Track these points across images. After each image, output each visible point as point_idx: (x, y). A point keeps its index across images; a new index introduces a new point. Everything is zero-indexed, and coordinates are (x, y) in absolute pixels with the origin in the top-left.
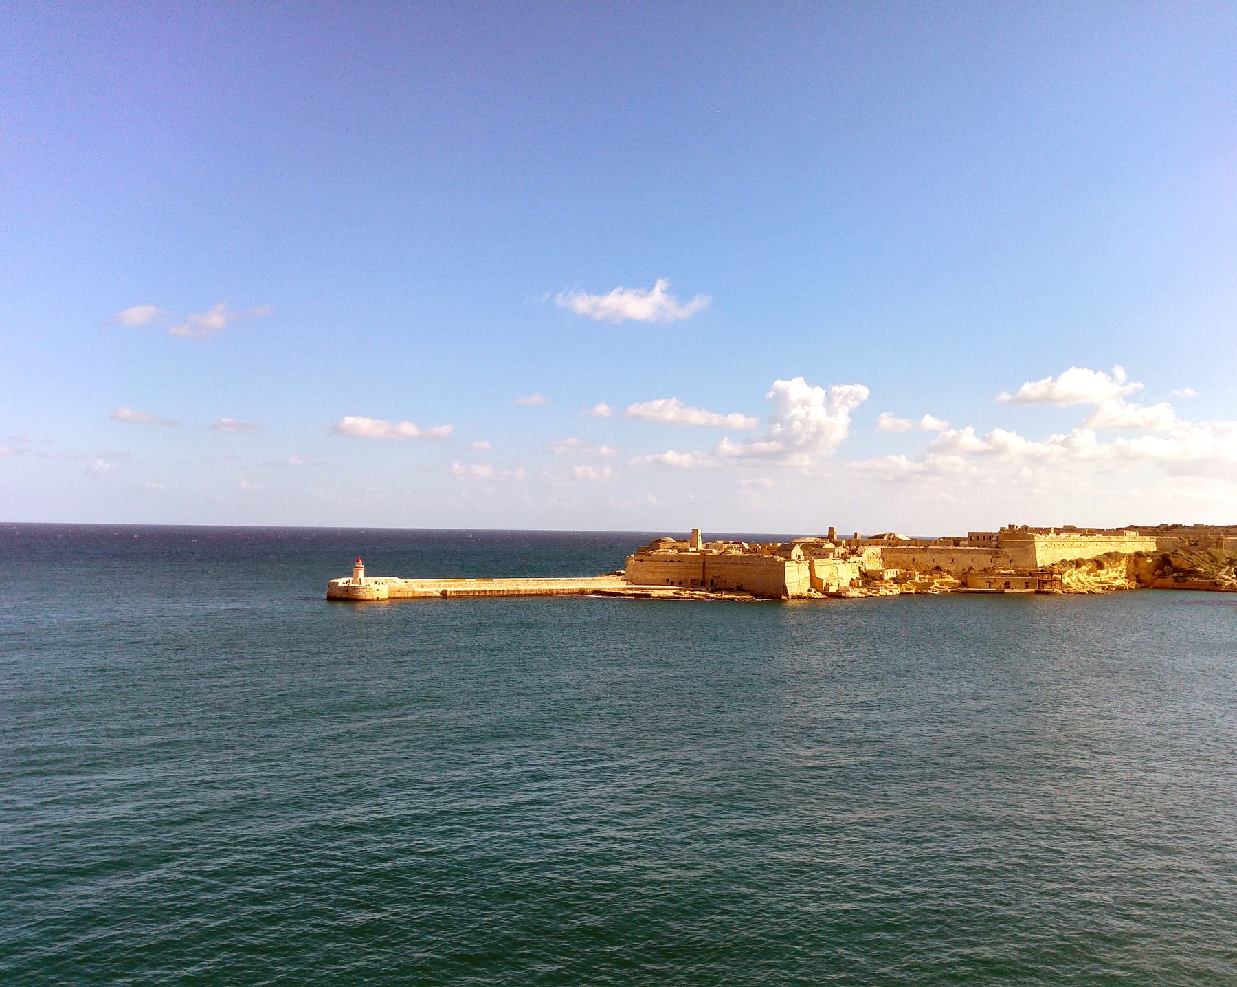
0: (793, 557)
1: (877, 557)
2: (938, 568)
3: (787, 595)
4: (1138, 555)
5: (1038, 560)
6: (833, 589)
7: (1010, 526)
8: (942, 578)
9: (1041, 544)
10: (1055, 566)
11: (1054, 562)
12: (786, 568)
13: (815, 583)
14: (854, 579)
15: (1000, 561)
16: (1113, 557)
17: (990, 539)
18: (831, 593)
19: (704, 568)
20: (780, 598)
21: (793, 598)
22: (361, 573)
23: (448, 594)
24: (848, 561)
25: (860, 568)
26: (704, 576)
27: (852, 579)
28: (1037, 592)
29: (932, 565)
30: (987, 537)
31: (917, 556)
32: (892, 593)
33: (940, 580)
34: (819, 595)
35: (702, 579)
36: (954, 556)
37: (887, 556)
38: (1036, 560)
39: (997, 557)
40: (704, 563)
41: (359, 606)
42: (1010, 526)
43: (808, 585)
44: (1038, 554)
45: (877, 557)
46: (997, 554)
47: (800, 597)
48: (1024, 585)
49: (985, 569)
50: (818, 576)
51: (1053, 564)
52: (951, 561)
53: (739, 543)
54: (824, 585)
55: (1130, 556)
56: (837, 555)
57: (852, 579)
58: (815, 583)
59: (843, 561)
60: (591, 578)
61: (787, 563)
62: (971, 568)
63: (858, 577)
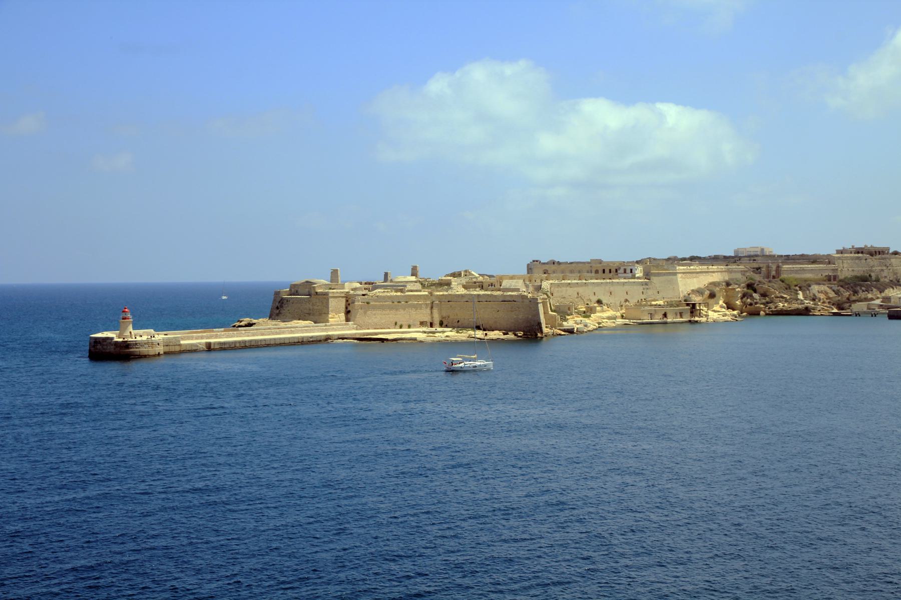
15: (650, 292)
17: (616, 271)
22: (130, 328)
23: (212, 347)
26: (432, 318)
30: (613, 270)
31: (581, 290)
35: (427, 319)
36: (612, 289)
39: (647, 289)
41: (135, 366)
60: (324, 324)
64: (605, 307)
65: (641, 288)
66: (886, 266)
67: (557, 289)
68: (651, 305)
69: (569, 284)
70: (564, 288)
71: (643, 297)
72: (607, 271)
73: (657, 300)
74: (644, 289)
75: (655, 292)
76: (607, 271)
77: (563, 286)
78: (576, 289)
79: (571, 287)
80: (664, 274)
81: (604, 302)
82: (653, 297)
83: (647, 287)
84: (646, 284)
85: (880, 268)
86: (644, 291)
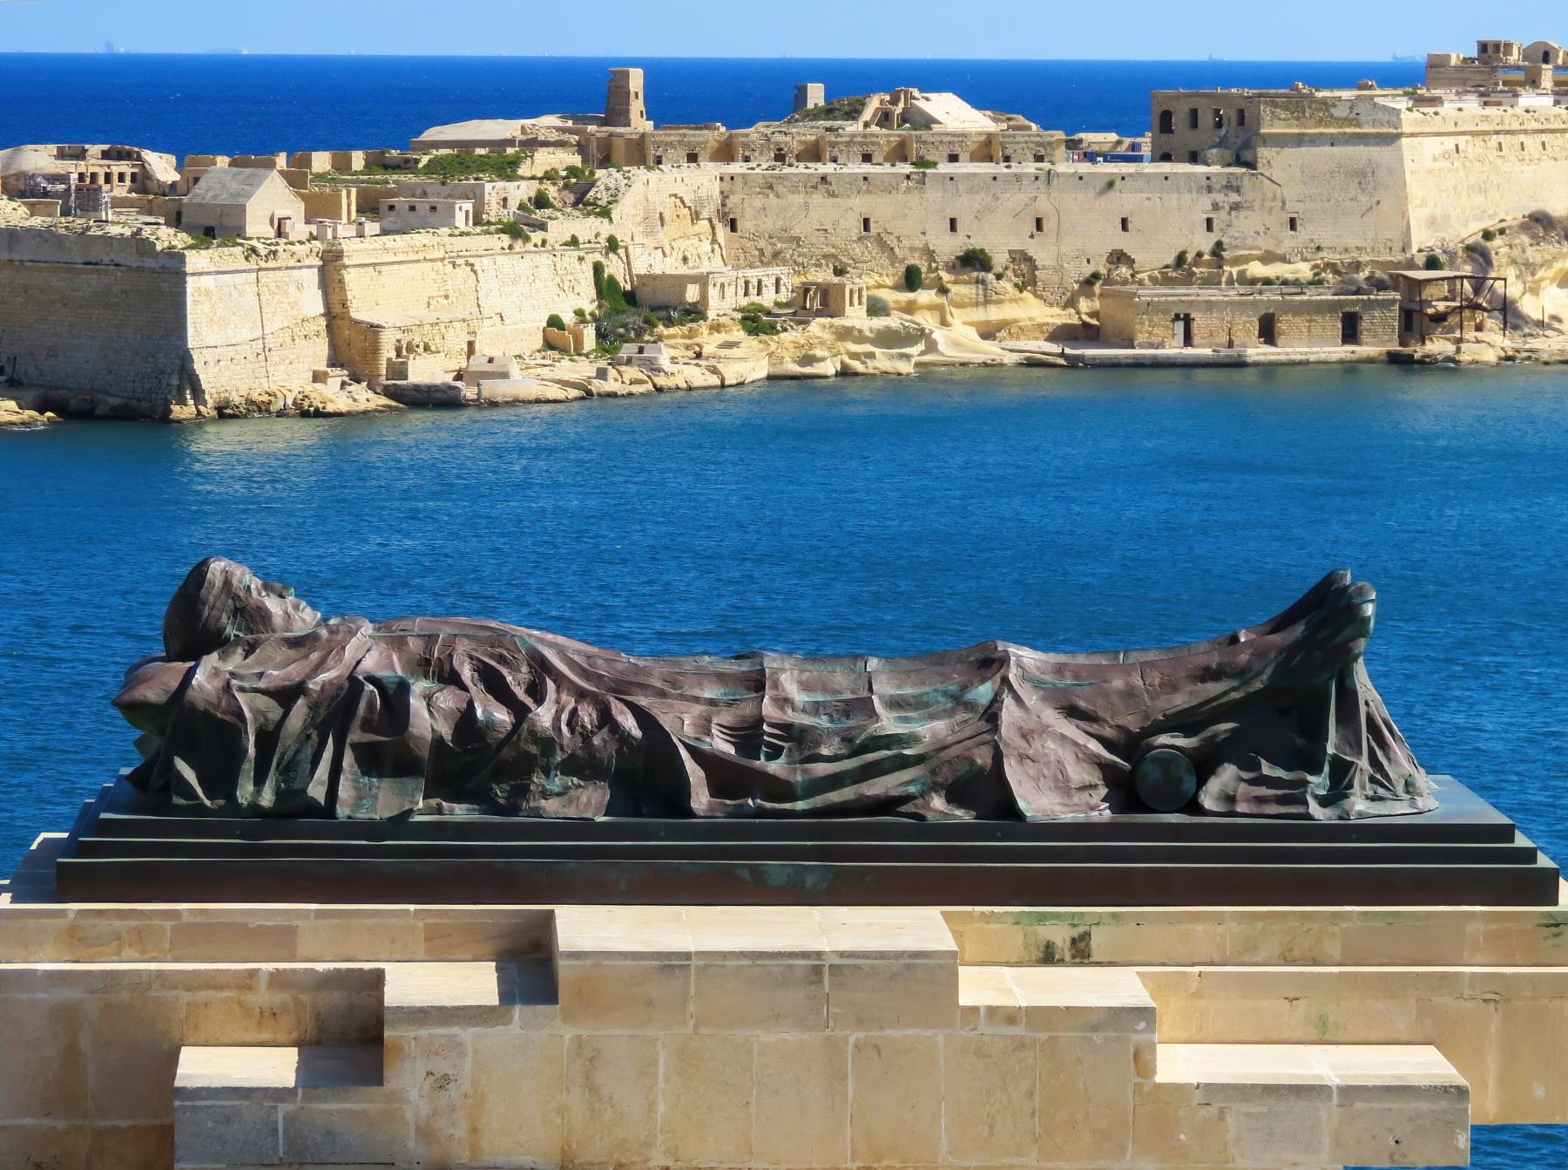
0: (257, 226)
1: (696, 217)
2: (973, 261)
3: (198, 394)
5: (1416, 215)
6: (424, 372)
7: (1483, 47)
8: (987, 302)
9: (1433, 146)
10: (1498, 242)
11: (1491, 224)
12: (191, 282)
14: (568, 318)
18: (417, 388)
20: (165, 418)
21: (224, 413)
24: (536, 237)
25: (598, 269)
27: (554, 322)
28: (1394, 359)
29: (949, 246)
30: (1228, 113)
31: (882, 208)
32: (715, 381)
33: (979, 315)
34: (364, 398)
36: (1043, 206)
38: (1404, 214)
39: (1235, 207)
42: (1483, 47)
43: (320, 349)
44: (1416, 188)
45: (696, 217)
46: (1238, 190)
47: (258, 409)
49: (1181, 259)
50: (361, 311)
51: (1488, 235)
52: (1032, 227)
53: (127, 156)
54: (388, 352)
56: (493, 211)
57: (554, 322)
59: (506, 239)
61: (196, 260)
62: (1119, 258)
63: (589, 307)
65: (1205, 202)
67: (758, 202)
68: (1243, 279)
69: (824, 179)
70: (799, 199)
72: (1206, 119)
73: (1283, 259)
74: (1216, 207)
75: (1278, 220)
76: (1206, 119)
77: (794, 190)
78: (860, 204)
79: (833, 195)
80: (1333, 141)
81: (999, 259)
82: (1265, 244)
83: (1234, 197)
86: (1219, 219)
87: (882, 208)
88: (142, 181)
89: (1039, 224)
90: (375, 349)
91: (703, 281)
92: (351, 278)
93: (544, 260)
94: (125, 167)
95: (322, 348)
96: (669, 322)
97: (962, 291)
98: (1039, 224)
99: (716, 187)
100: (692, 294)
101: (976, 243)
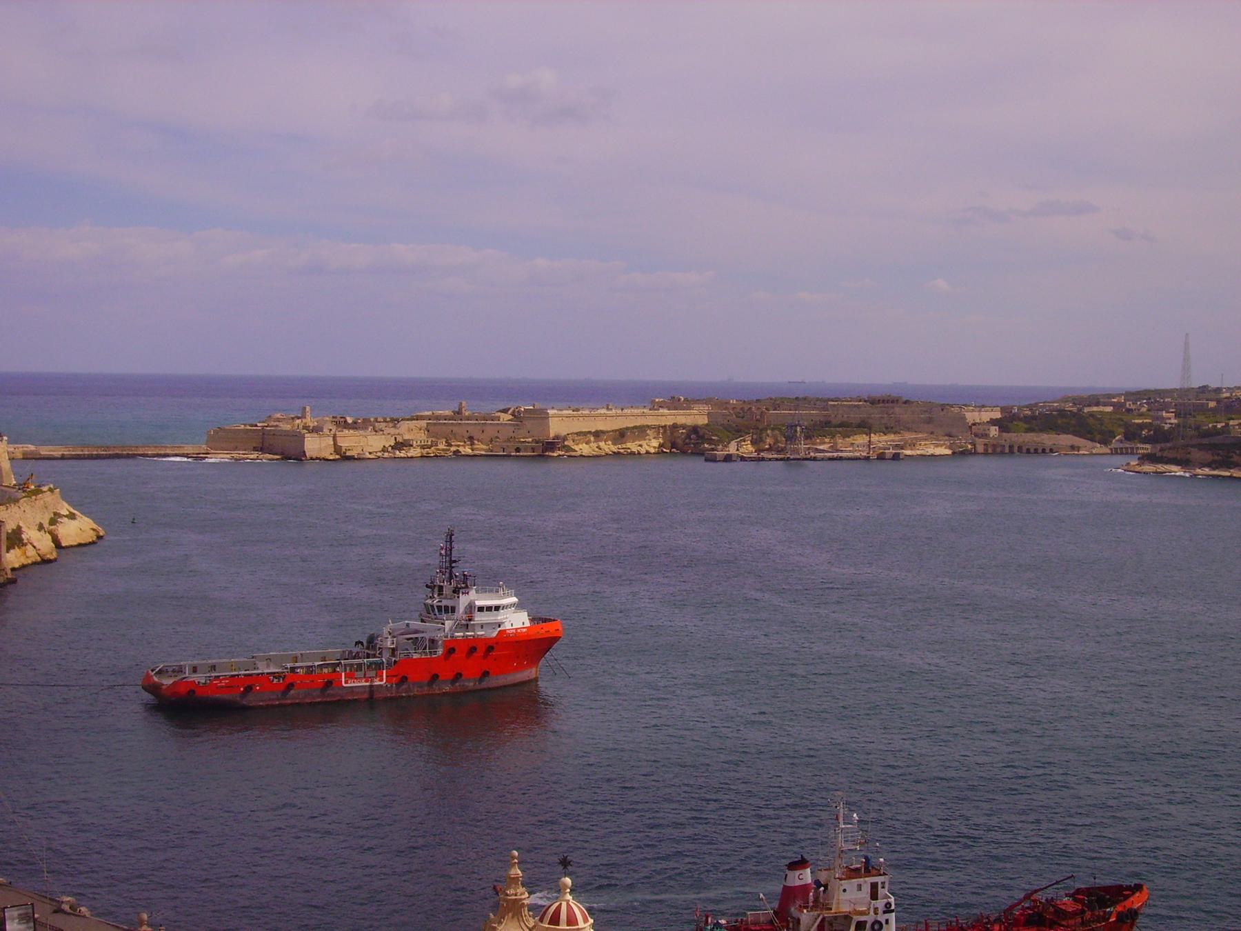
2: (471, 438)
3: (306, 456)
4: (675, 427)
13: (337, 449)
14: (387, 446)
16: (640, 431)
19: (263, 438)
25: (395, 438)
26: (263, 444)
27: (384, 446)
35: (261, 445)
37: (431, 428)
40: (263, 434)
45: (420, 430)
48: (531, 450)
51: (568, 434)
55: (665, 427)
57: (384, 446)
58: (337, 449)
61: (306, 435)
64: (476, 442)
66: (887, 414)
71: (513, 435)
78: (451, 428)
84: (517, 425)
85: (880, 416)
87: (455, 429)
88: (346, 421)
89: (483, 431)
90: (341, 450)
91: (412, 440)
92: (338, 439)
93: (383, 436)
94: (343, 420)
95: (333, 450)
96: (406, 447)
97: (469, 443)
98: (483, 431)
99: (425, 425)
100: (411, 443)
101: (472, 435)
